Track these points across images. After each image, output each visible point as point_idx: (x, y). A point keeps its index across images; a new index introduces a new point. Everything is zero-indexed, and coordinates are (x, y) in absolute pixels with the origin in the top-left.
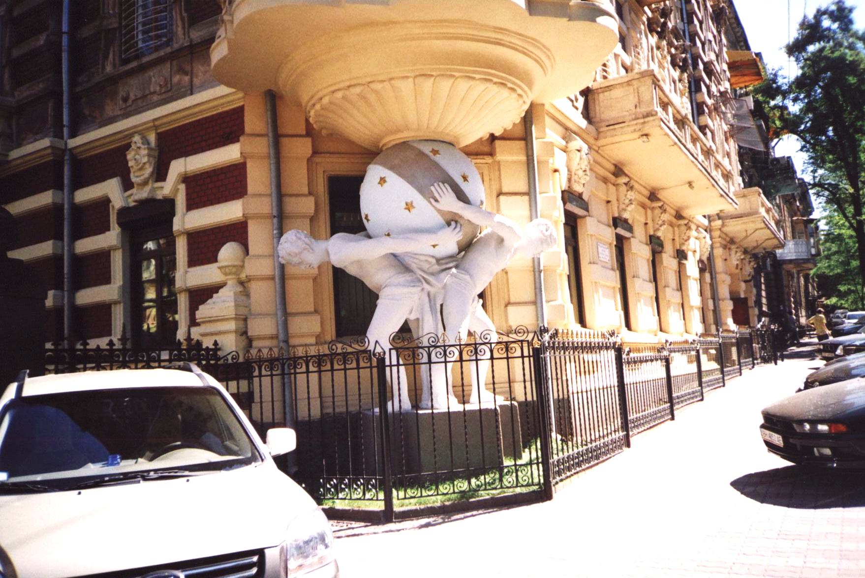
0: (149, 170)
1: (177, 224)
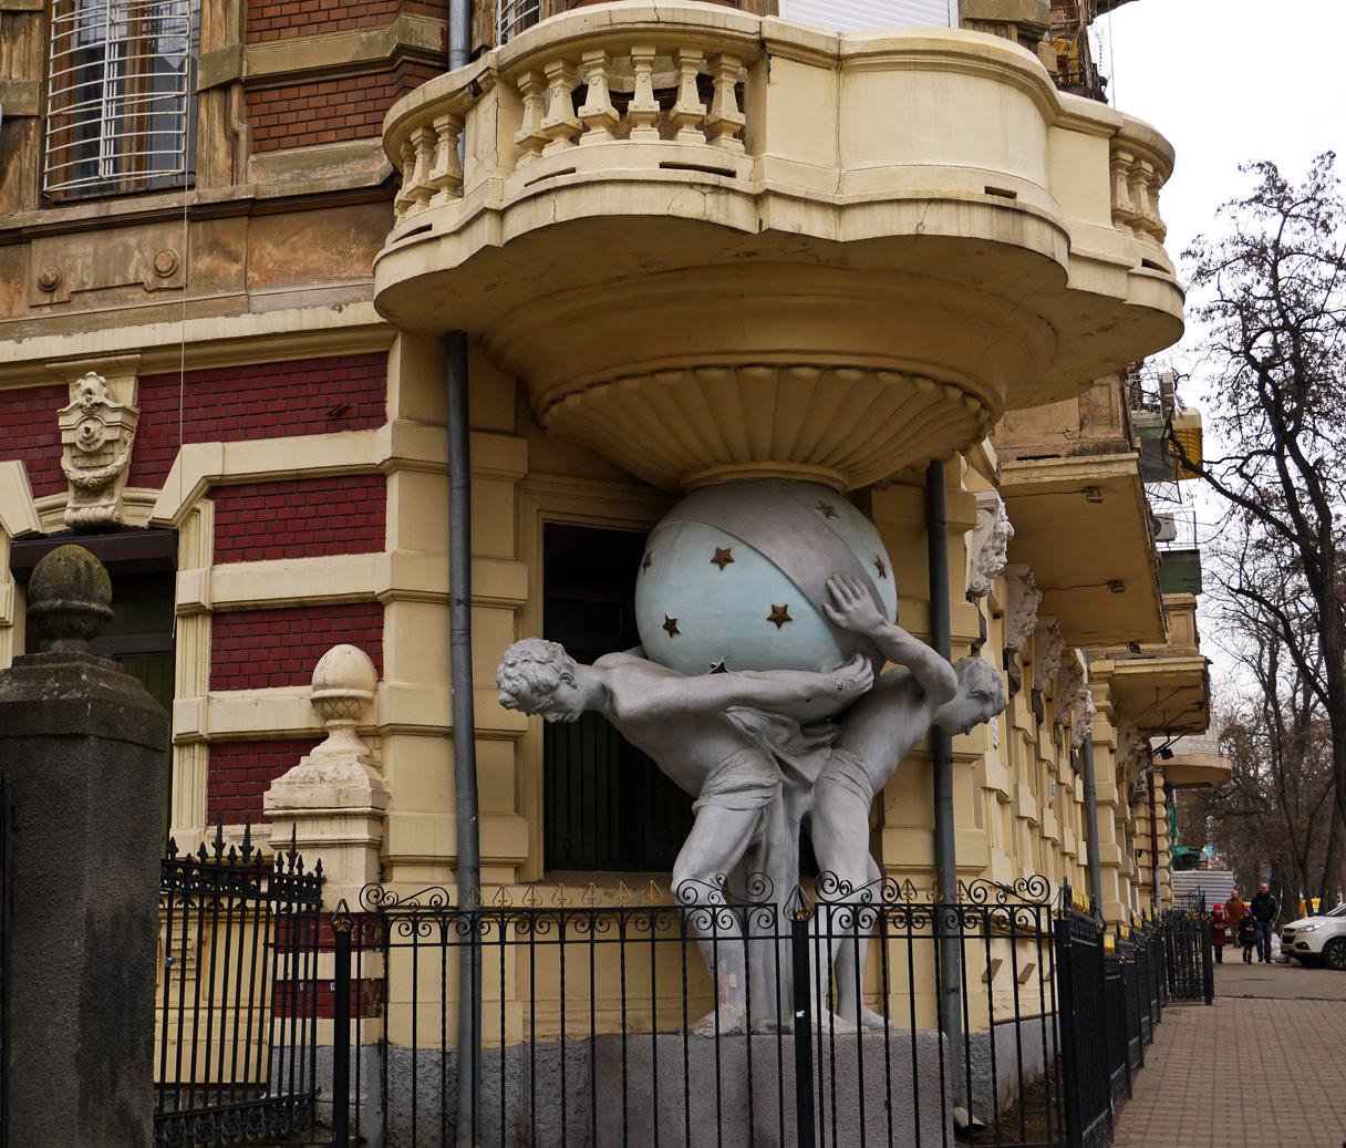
0: (121, 459)
1: (188, 588)
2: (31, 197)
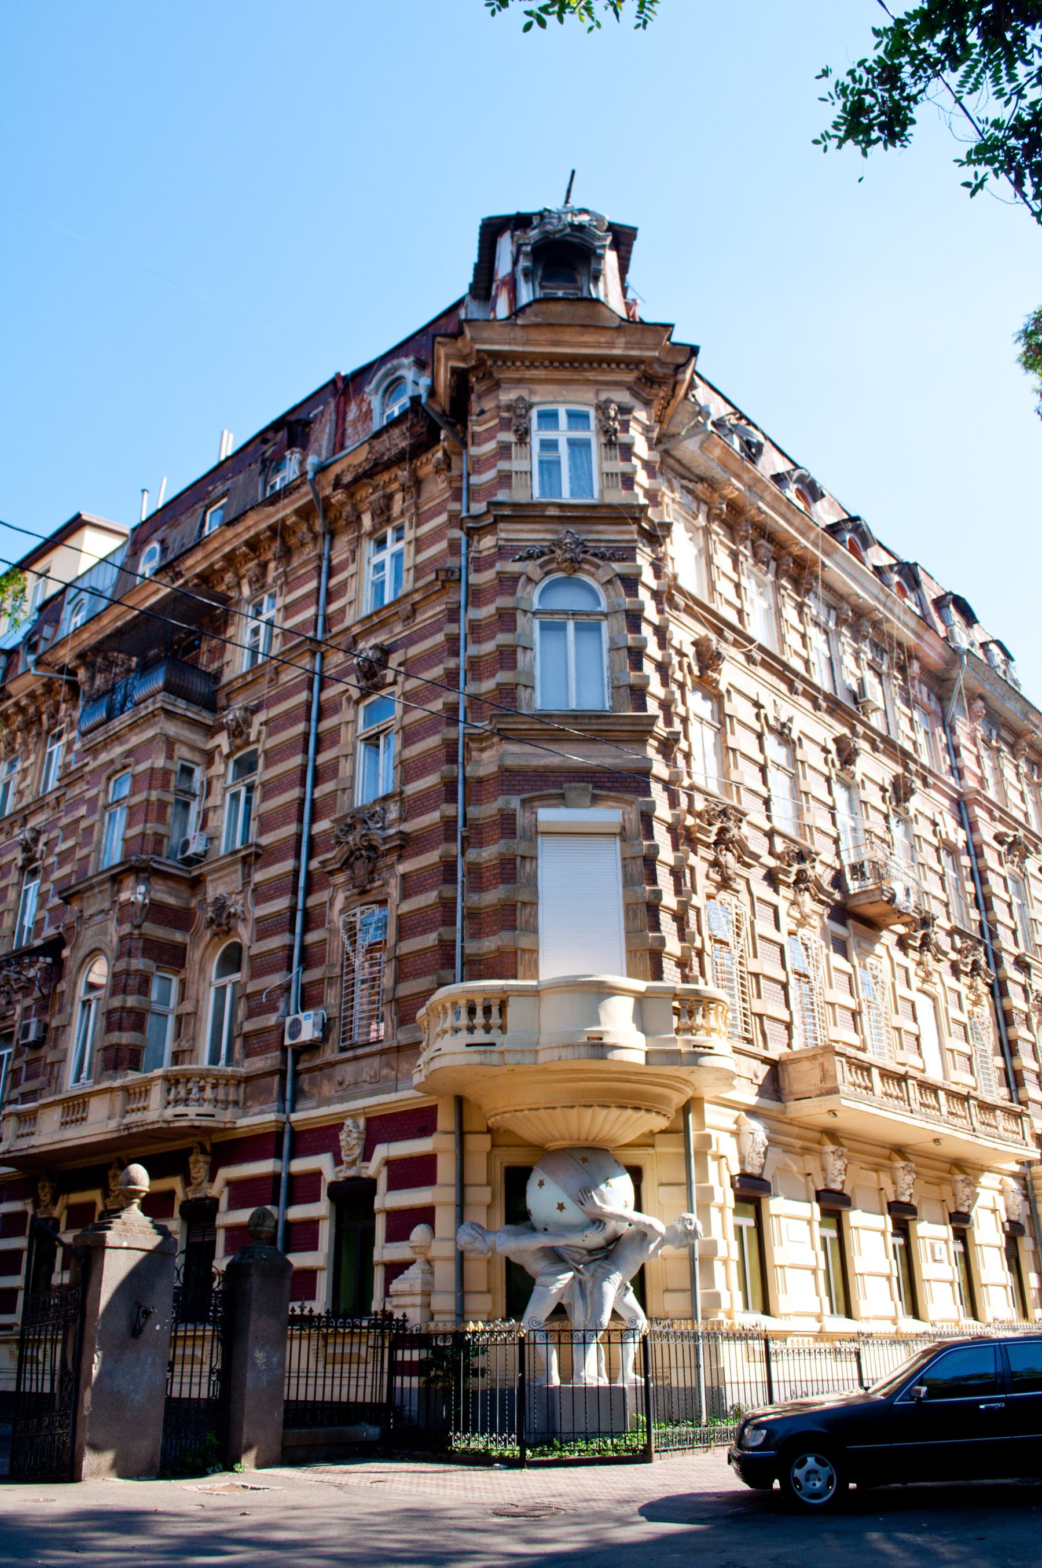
0: (358, 1151)
2: (336, 1049)
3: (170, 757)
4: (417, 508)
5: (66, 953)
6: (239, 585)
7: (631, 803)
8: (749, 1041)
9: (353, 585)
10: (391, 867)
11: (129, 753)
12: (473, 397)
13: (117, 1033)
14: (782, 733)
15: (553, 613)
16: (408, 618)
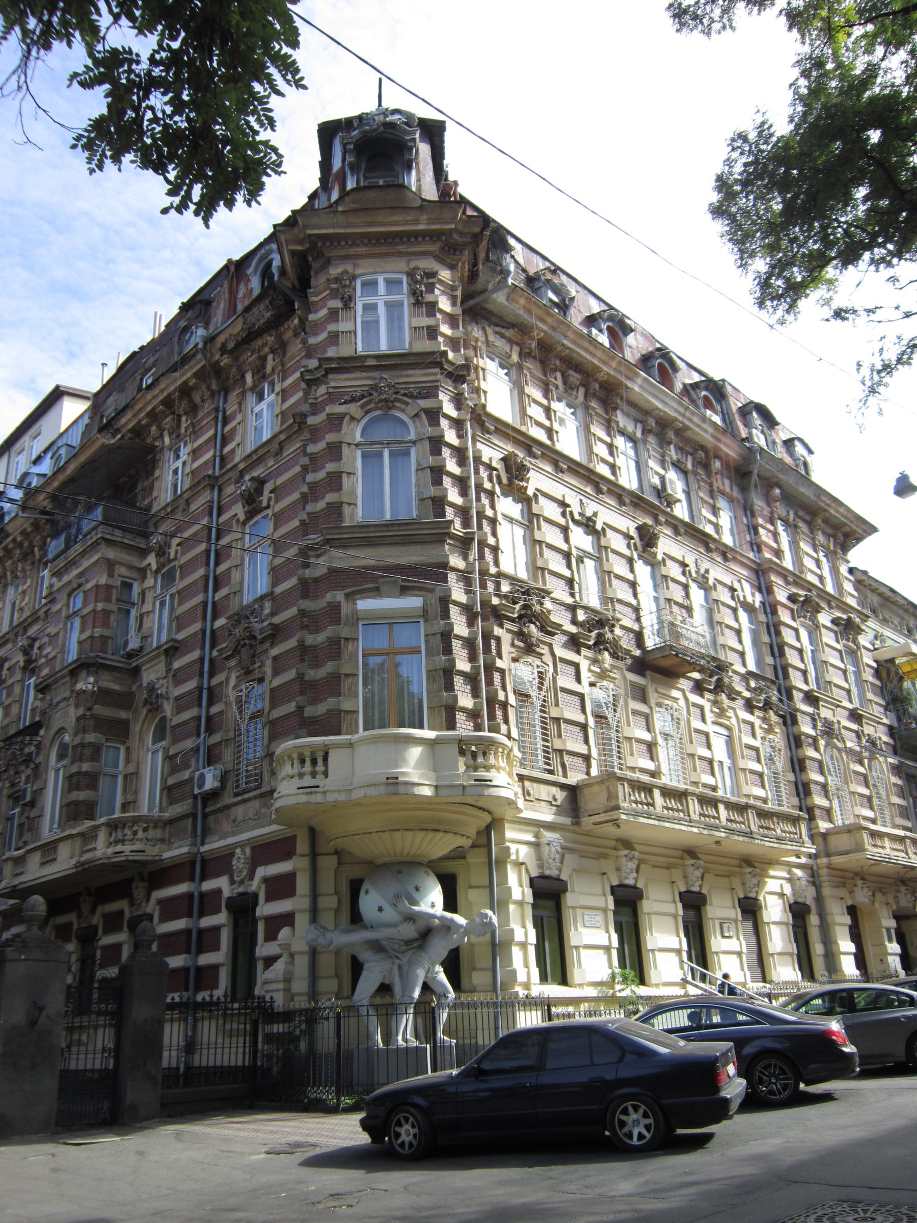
1: (258, 913)
3: (111, 575)
4: (283, 365)
5: (42, 732)
6: (161, 436)
7: (432, 591)
8: (551, 772)
9: (240, 430)
10: (266, 651)
11: (81, 574)
12: (312, 273)
13: (75, 793)
14: (588, 525)
15: (371, 444)
16: (277, 454)
